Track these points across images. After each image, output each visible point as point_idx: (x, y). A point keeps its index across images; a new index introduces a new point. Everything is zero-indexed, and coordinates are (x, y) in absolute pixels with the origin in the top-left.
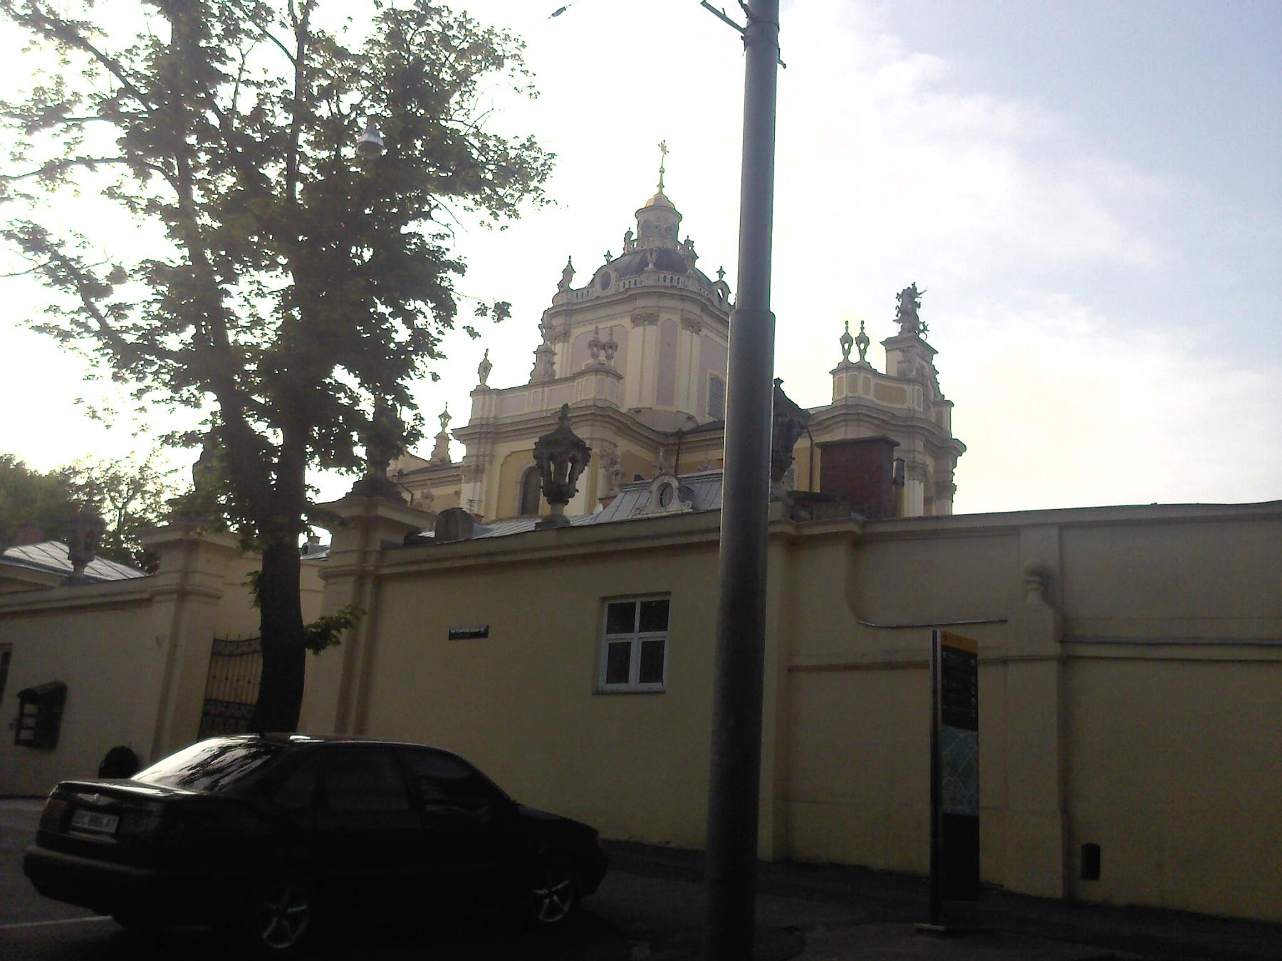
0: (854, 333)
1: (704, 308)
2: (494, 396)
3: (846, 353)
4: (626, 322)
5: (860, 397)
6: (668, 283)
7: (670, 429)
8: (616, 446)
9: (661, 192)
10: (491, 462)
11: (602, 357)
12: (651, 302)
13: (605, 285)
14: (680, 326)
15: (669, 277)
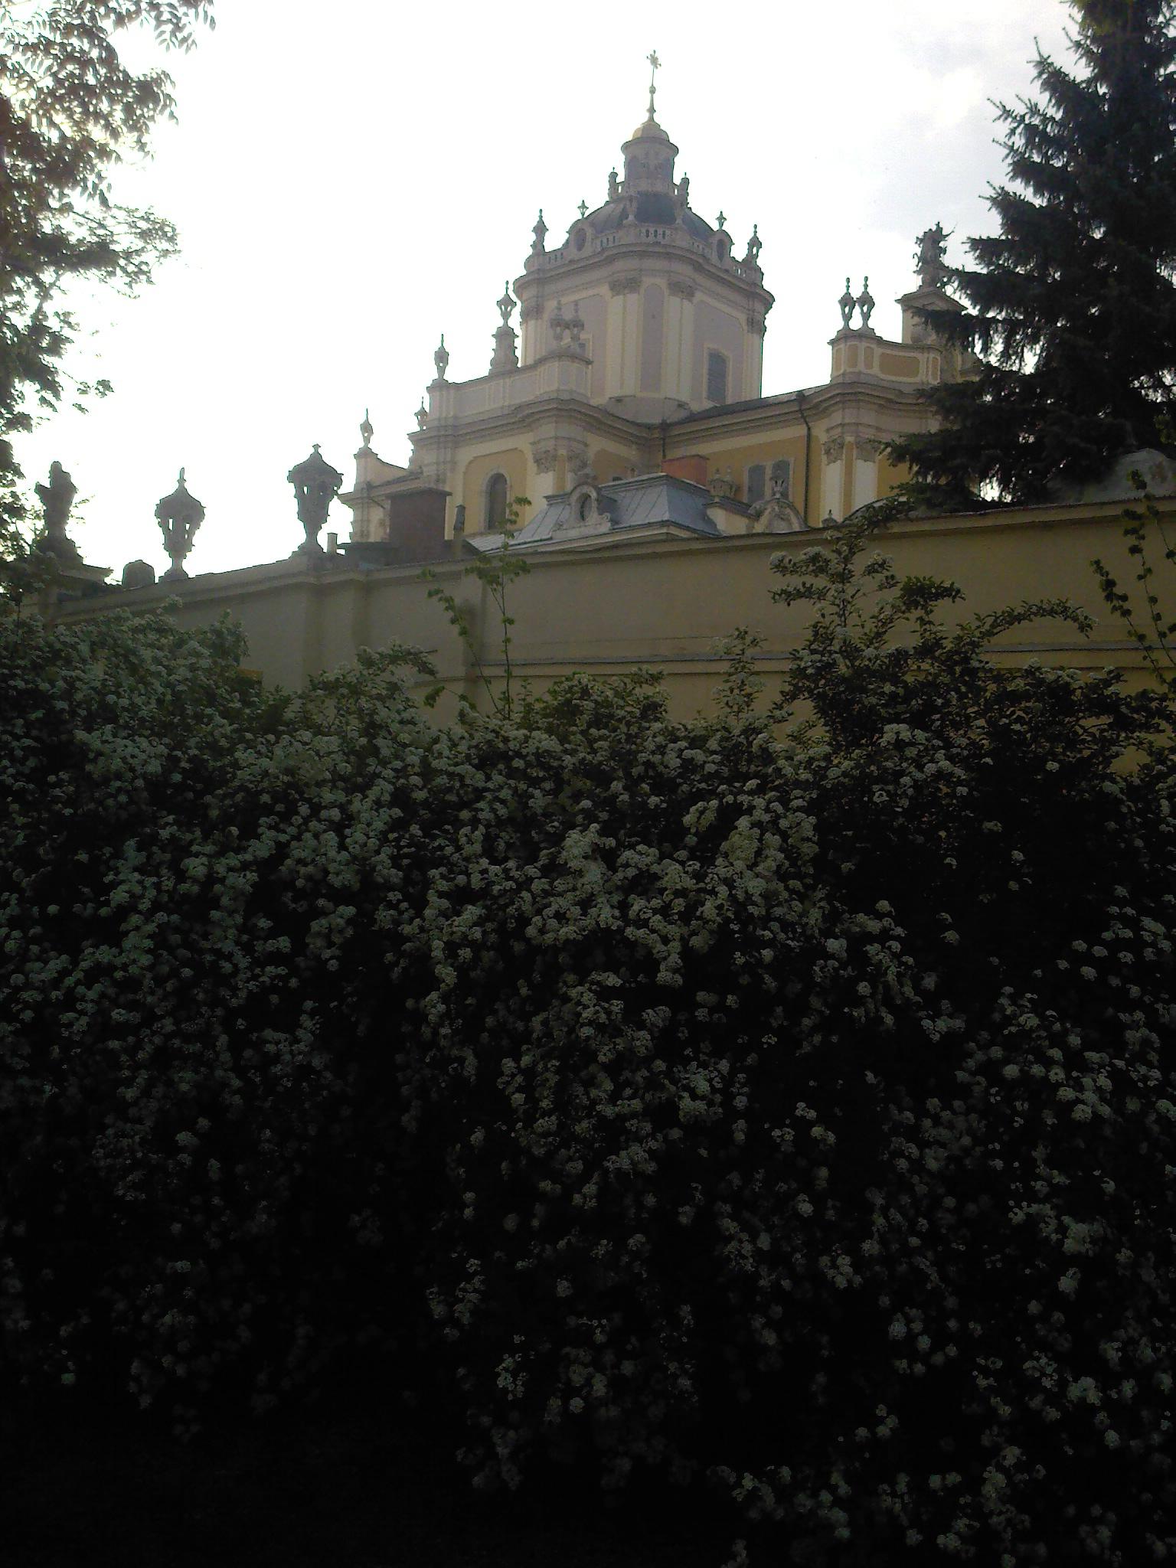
0: (856, 293)
1: (698, 268)
2: (452, 392)
3: (847, 317)
4: (604, 290)
5: (860, 373)
6: (651, 239)
7: (656, 420)
8: (586, 445)
9: (652, 119)
10: (453, 470)
11: (567, 340)
12: (632, 263)
13: (580, 247)
14: (666, 292)
15: (652, 230)
